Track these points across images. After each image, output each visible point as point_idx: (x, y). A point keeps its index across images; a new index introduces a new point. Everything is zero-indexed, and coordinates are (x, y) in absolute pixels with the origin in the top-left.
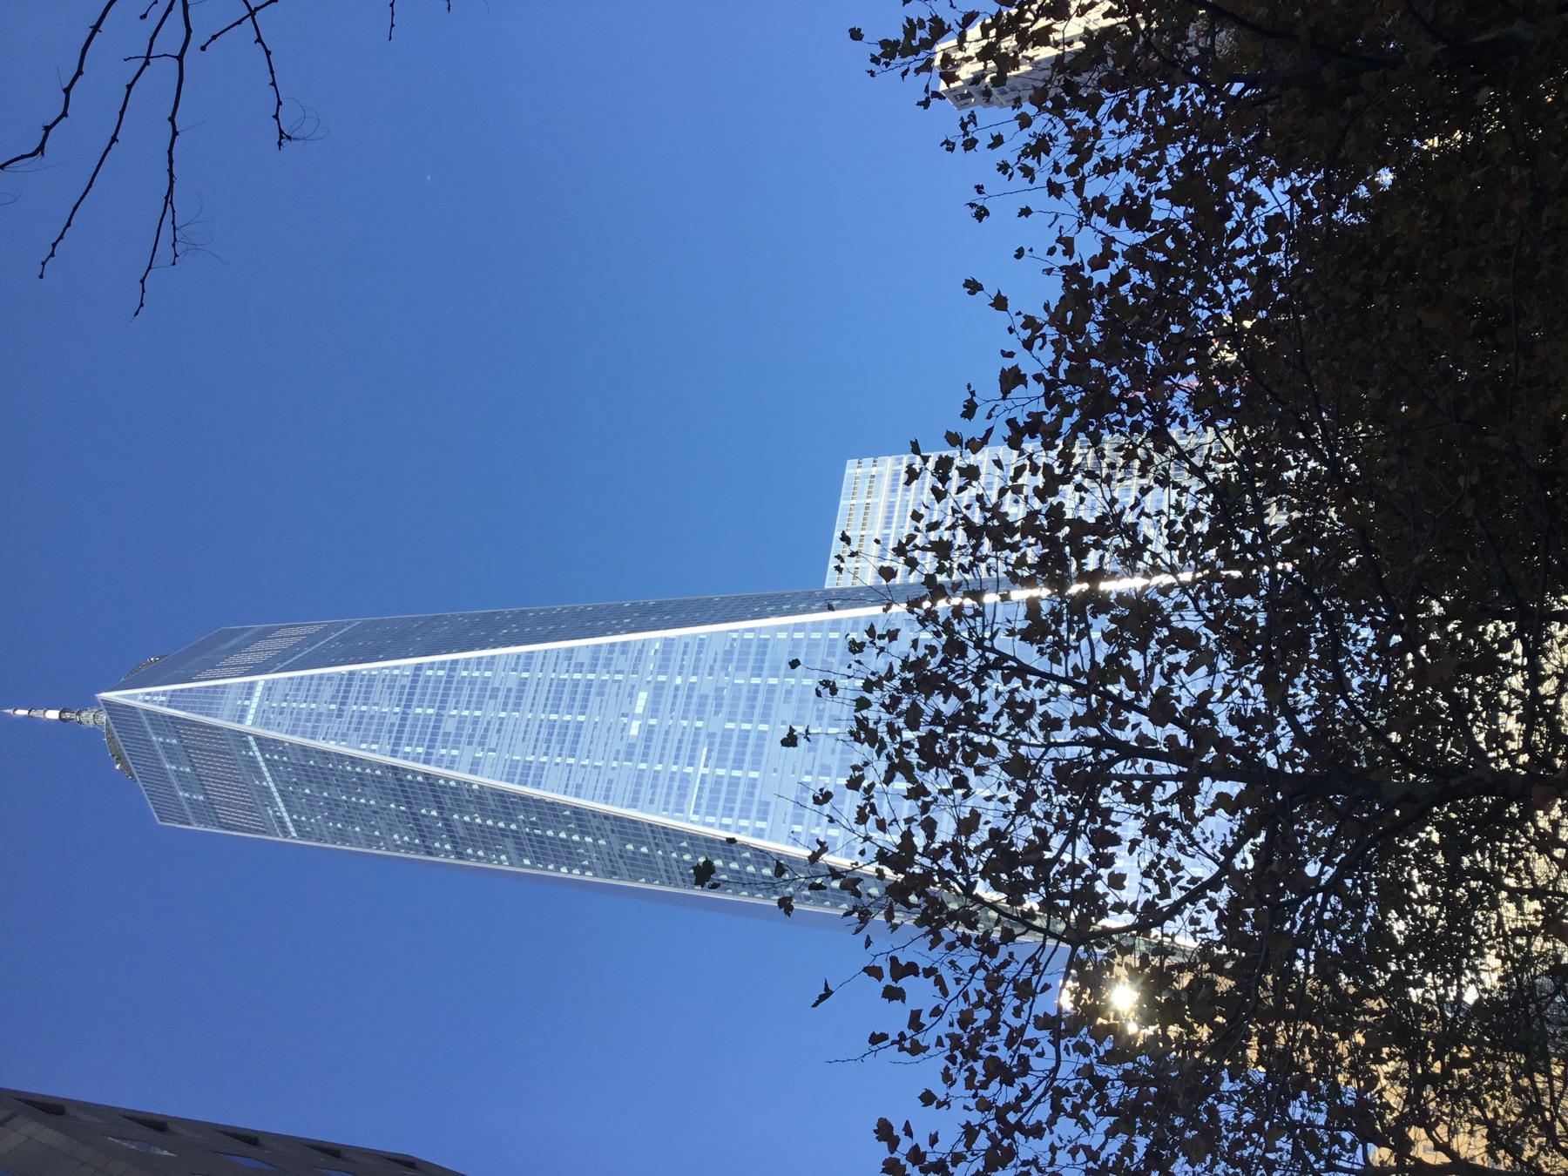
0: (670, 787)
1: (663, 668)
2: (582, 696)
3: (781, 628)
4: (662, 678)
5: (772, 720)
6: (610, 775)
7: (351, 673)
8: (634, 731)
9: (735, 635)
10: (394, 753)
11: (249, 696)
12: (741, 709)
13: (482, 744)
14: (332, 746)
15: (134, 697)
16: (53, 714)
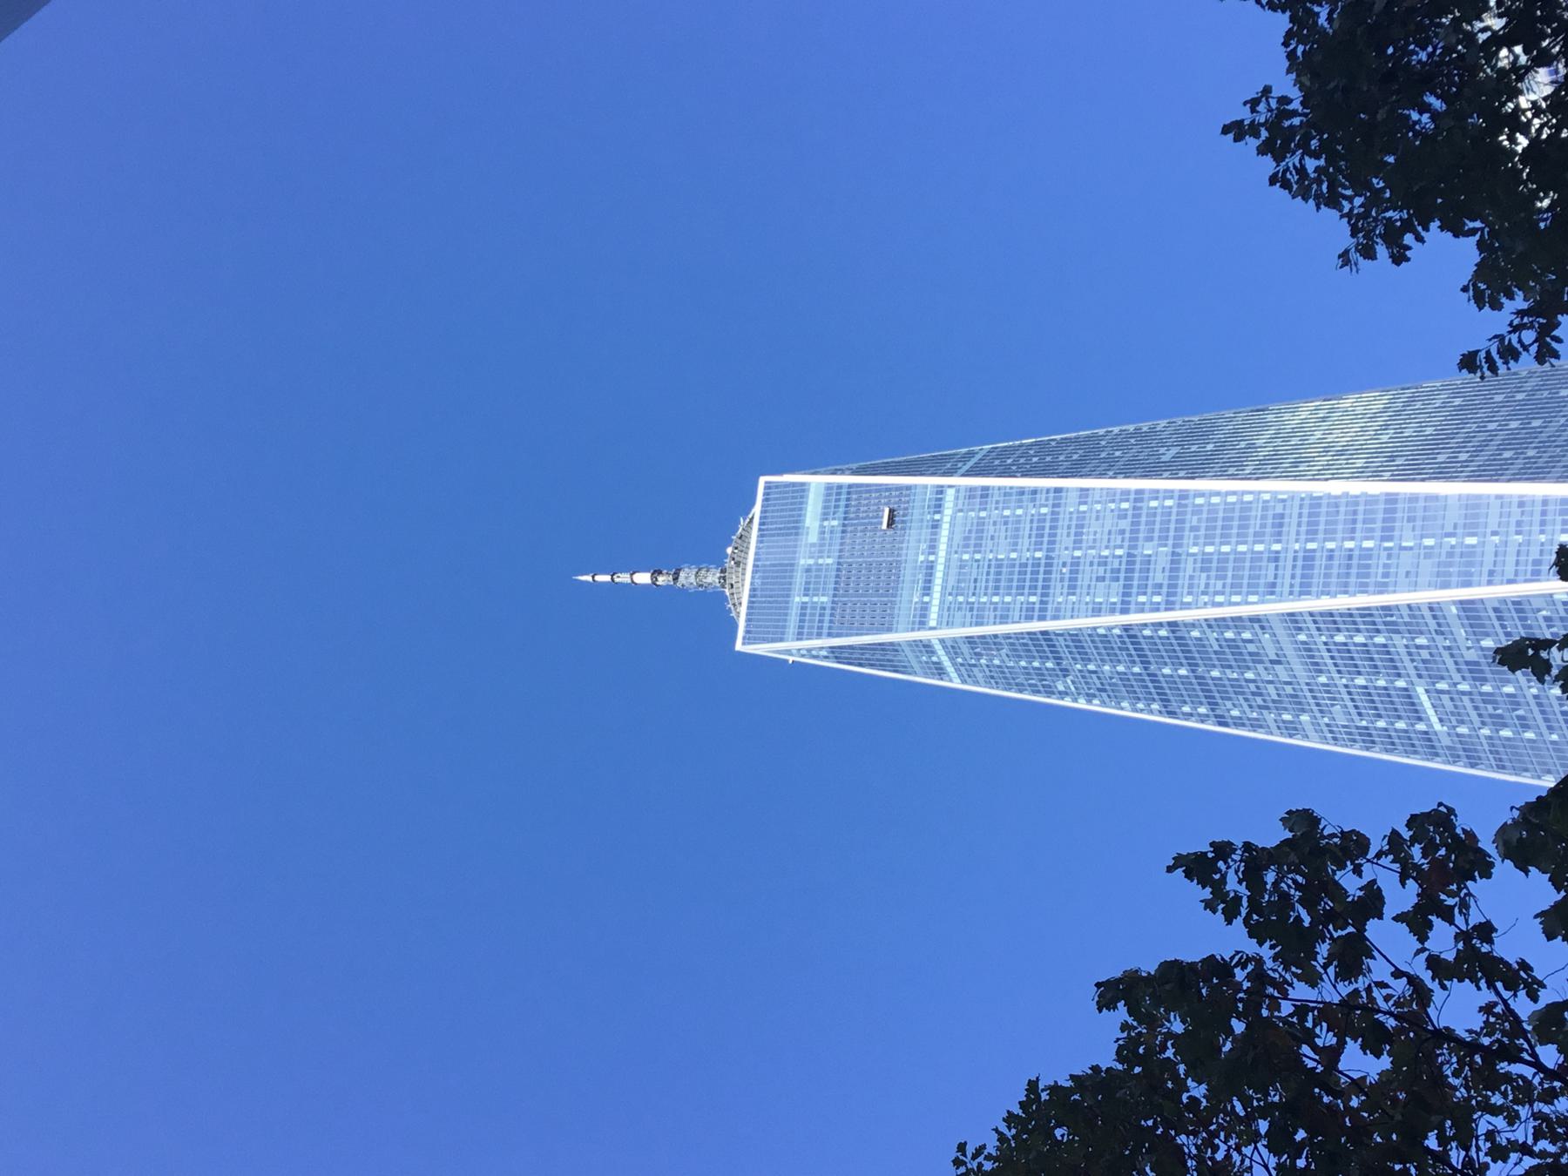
7: (1044, 633)
10: (1172, 714)
14: (1082, 704)
15: (788, 652)
16: (643, 578)
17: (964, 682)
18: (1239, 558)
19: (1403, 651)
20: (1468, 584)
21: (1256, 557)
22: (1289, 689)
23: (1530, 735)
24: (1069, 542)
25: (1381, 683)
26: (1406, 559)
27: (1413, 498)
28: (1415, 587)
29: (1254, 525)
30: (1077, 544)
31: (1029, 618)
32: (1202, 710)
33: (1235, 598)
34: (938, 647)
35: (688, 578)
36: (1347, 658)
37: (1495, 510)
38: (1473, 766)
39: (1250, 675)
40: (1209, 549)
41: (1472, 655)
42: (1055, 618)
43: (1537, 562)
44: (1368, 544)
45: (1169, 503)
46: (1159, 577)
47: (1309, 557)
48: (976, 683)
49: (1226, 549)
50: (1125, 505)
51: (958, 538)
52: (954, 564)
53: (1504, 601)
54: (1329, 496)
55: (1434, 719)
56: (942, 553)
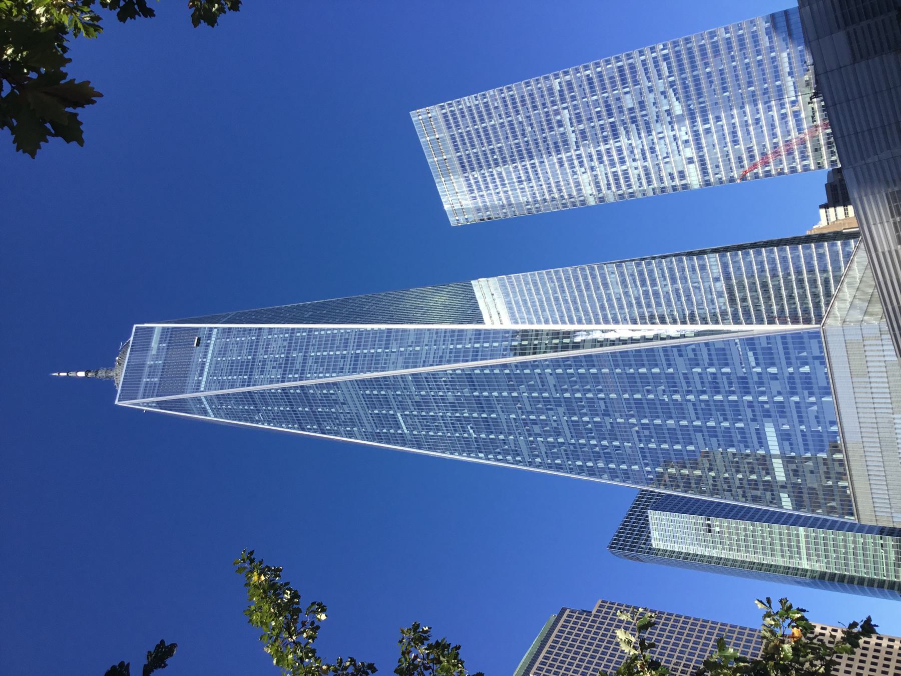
7: (249, 392)
10: (303, 429)
11: (202, 403)
14: (266, 426)
15: (138, 404)
16: (81, 374)
17: (216, 417)
18: (330, 357)
19: (392, 397)
20: (415, 367)
21: (336, 357)
22: (349, 416)
23: (440, 434)
24: (262, 352)
25: (384, 412)
26: (393, 356)
27: (397, 330)
28: (395, 368)
29: (337, 342)
30: (266, 352)
31: (243, 386)
32: (315, 427)
33: (327, 375)
34: (204, 400)
35: (102, 374)
36: (371, 402)
37: (427, 336)
38: (419, 448)
39: (333, 410)
40: (319, 354)
41: (417, 399)
42: (254, 385)
43: (441, 357)
44: (380, 350)
45: (304, 334)
46: (298, 366)
47: (357, 356)
48: (221, 417)
49: (325, 353)
50: (287, 335)
51: (216, 350)
52: (214, 362)
53: (428, 374)
54: (366, 330)
55: (404, 428)
56: (209, 358)
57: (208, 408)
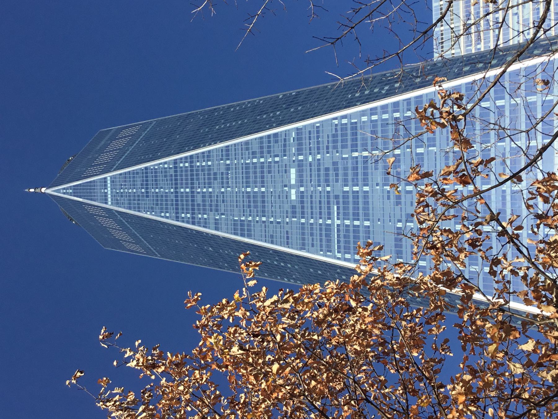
0: (321, 235)
1: (300, 151)
2: (260, 174)
3: (363, 113)
4: (301, 158)
5: (370, 183)
6: (287, 228)
7: (146, 168)
8: (293, 197)
9: (336, 122)
10: (177, 219)
11: (106, 187)
12: (350, 177)
13: (217, 210)
14: (148, 216)
15: (58, 191)
57: (109, 192)
